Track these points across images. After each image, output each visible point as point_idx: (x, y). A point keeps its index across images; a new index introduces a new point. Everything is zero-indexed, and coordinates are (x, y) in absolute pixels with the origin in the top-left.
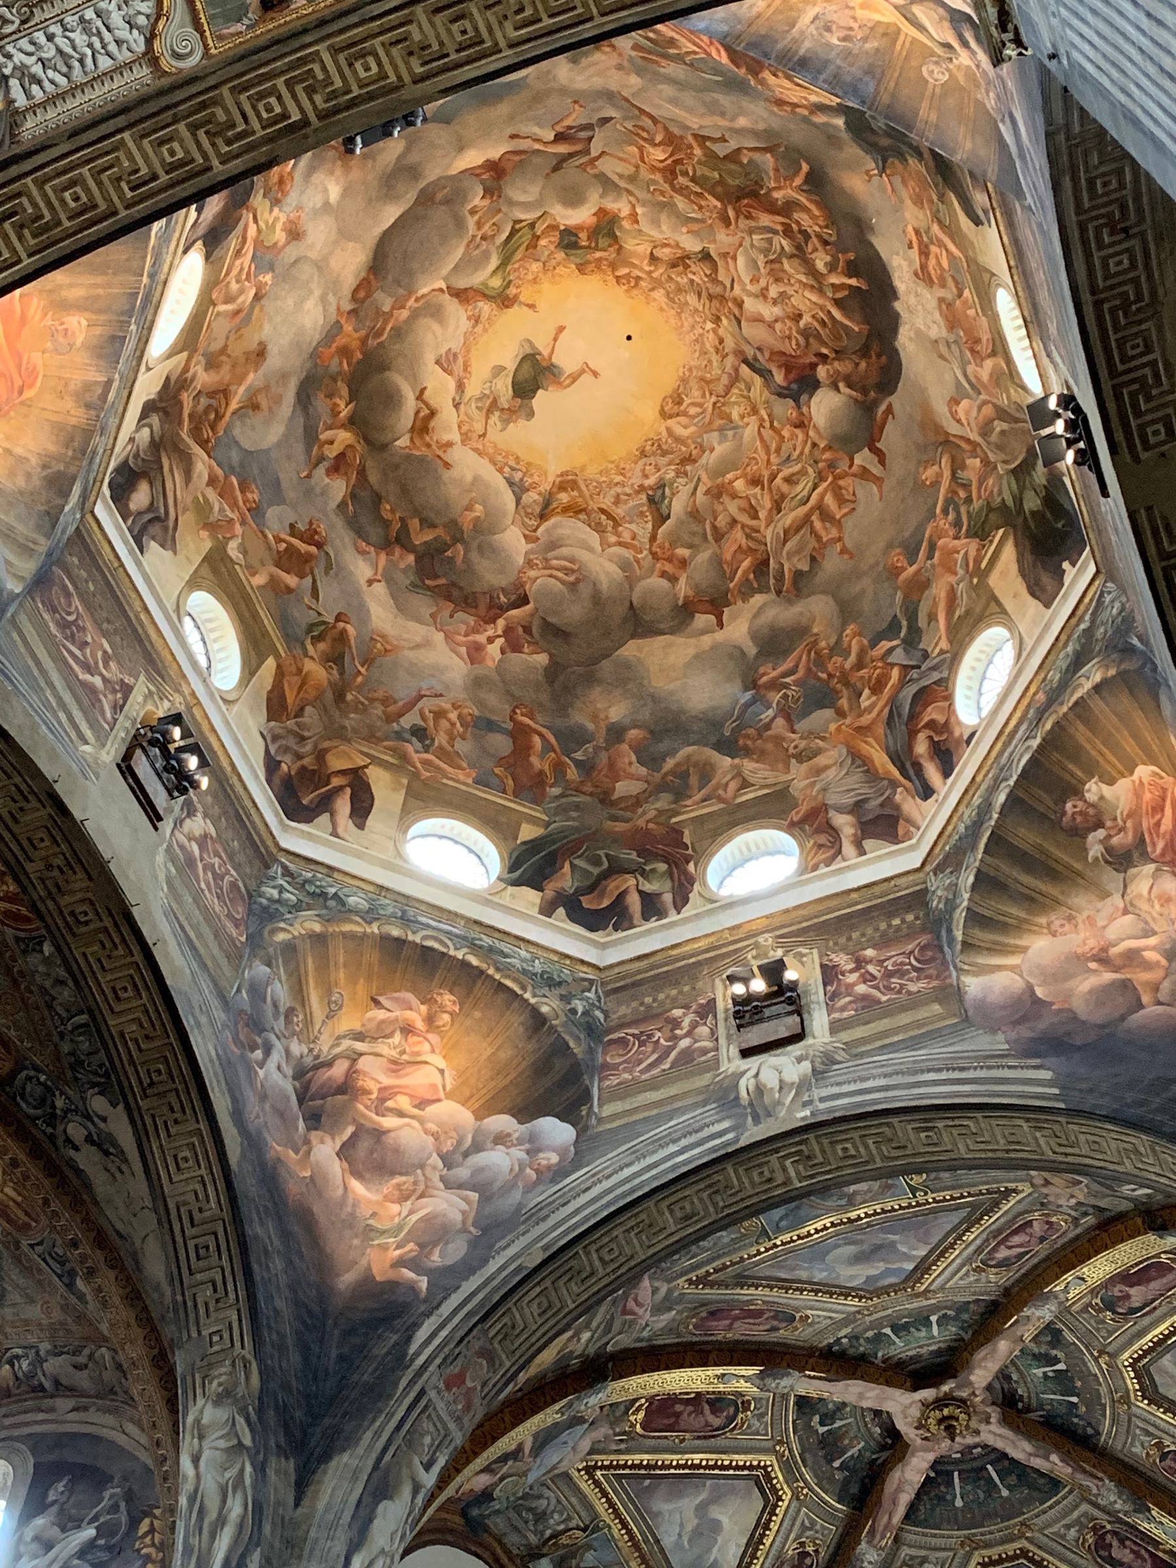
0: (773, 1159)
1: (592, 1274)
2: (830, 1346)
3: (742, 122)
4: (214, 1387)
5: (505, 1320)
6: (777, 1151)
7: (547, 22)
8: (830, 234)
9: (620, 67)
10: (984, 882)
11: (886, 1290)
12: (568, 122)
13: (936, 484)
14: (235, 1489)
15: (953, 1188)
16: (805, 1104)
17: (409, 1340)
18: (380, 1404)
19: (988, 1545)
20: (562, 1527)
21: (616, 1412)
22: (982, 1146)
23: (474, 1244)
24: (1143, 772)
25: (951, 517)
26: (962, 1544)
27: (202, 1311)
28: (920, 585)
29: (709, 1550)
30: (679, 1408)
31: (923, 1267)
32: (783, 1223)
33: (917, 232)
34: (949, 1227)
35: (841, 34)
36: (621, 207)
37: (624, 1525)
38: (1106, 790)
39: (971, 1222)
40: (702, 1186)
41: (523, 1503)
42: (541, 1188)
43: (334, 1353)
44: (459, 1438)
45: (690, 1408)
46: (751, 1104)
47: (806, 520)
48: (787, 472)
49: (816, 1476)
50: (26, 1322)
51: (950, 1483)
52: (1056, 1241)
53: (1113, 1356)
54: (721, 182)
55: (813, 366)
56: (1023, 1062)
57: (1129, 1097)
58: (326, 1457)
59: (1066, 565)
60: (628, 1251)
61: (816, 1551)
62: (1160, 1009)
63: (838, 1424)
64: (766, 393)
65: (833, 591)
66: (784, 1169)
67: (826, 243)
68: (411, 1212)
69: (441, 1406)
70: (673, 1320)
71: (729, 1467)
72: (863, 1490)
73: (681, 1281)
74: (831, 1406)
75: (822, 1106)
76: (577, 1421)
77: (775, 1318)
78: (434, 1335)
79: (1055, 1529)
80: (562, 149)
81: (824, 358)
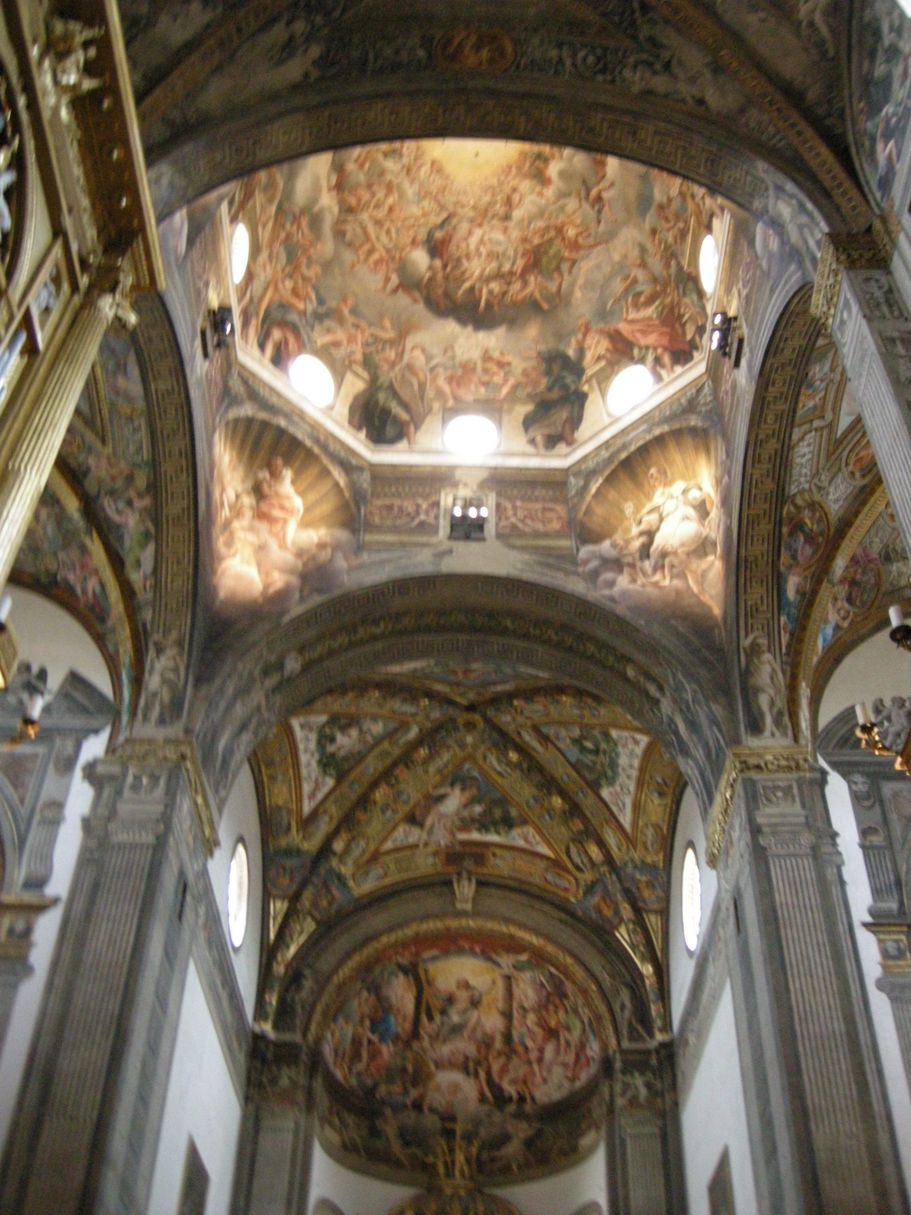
3: (578, 294)
7: (754, 491)
8: (508, 299)
9: (625, 256)
10: (250, 421)
12: (606, 208)
13: (383, 328)
25: (370, 340)
28: (341, 320)
33: (509, 364)
35: (655, 475)
36: (550, 192)
47: (368, 238)
48: (393, 230)
54: (546, 253)
55: (441, 257)
59: (364, 432)
64: (430, 225)
65: (337, 256)
67: (504, 294)
80: (594, 192)
81: (445, 266)
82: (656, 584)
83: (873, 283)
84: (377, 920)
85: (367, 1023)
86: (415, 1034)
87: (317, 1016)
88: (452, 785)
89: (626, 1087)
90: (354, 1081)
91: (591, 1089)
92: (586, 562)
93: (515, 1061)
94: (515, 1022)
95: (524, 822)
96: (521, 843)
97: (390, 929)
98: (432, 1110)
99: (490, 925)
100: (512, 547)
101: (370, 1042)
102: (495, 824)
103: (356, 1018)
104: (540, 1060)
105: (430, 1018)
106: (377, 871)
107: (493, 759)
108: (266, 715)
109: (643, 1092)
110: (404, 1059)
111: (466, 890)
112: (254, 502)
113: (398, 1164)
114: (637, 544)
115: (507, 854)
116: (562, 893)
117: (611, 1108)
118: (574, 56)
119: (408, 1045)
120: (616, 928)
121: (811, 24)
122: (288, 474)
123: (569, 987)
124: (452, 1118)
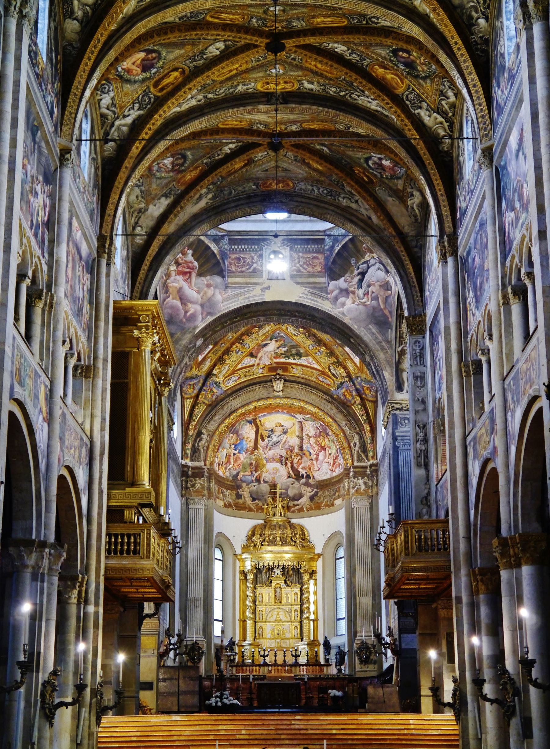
24: (196, 264)
38: (190, 255)
50: (151, 184)
82: (364, 304)
83: (417, 344)
84: (235, 402)
85: (233, 446)
86: (256, 447)
87: (210, 452)
88: (271, 340)
89: (356, 484)
90: (227, 474)
91: (339, 480)
92: (332, 291)
93: (305, 459)
94: (304, 441)
95: (307, 355)
96: (306, 364)
97: (243, 406)
98: (265, 482)
99: (290, 402)
100: (298, 283)
101: (234, 454)
102: (293, 355)
103: (228, 446)
104: (317, 459)
105: (263, 440)
106: (234, 378)
107: (291, 329)
108: (188, 363)
109: (363, 487)
110: (250, 459)
111: (278, 385)
112: (175, 268)
113: (250, 510)
114: (356, 279)
115: (300, 368)
116: (327, 386)
117: (348, 494)
118: (319, 189)
119: (252, 453)
120: (353, 405)
121: (412, 208)
122: (190, 252)
123: (330, 433)
124: (274, 486)
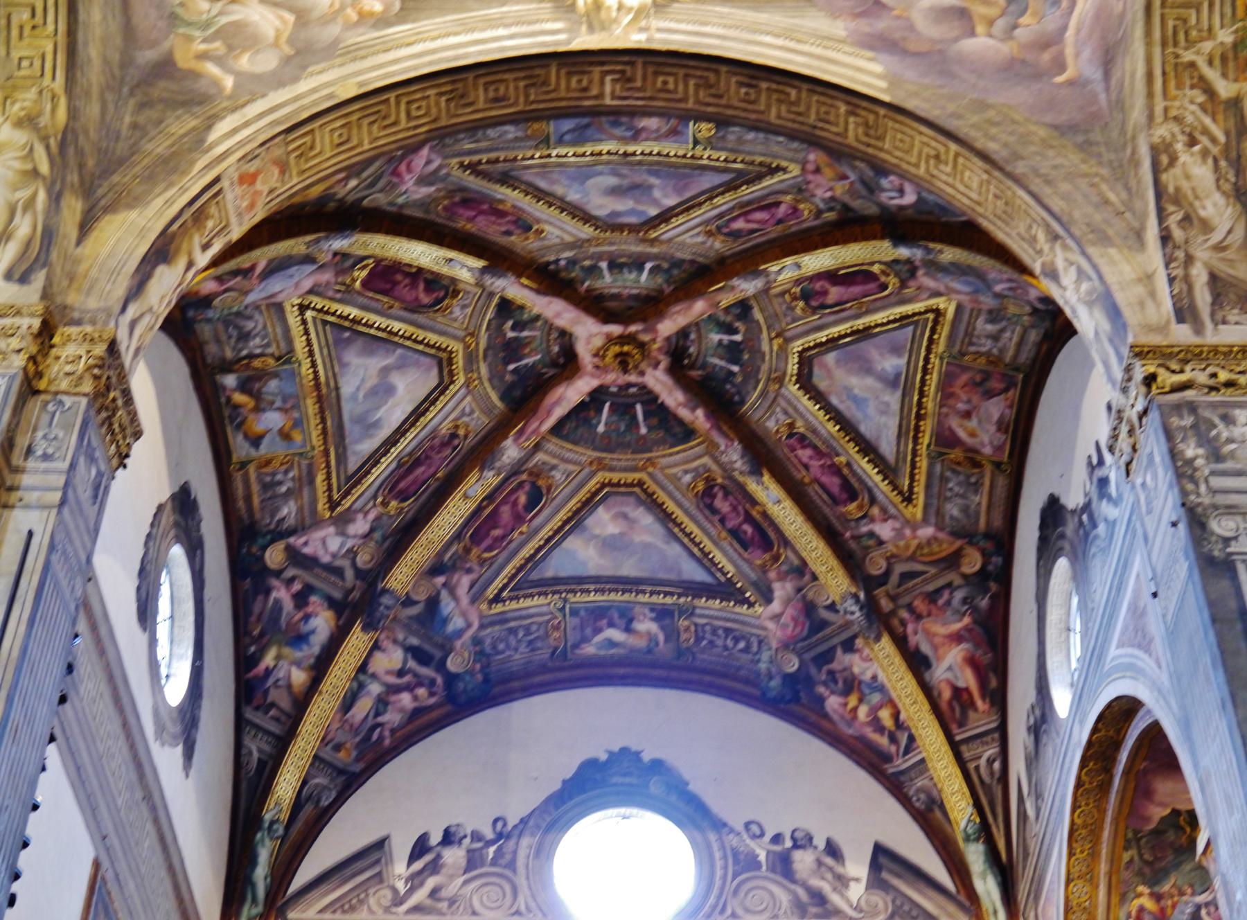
0: (597, 70)
1: (395, 124)
2: (548, 263)
4: (15, 109)
5: (307, 139)
6: (602, 64)
11: (620, 228)
14: (25, 210)
15: (732, 151)
16: (642, 30)
17: (209, 127)
18: (174, 177)
19: (612, 469)
20: (258, 351)
21: (344, 262)
22: (792, 116)
23: (287, 60)
26: (591, 463)
27: (15, 32)
29: (378, 408)
30: (399, 277)
31: (665, 216)
32: (567, 137)
34: (707, 185)
37: (314, 365)
39: (730, 187)
40: (522, 74)
41: (234, 320)
42: (361, 30)
43: (127, 119)
44: (236, 233)
45: (407, 281)
46: (587, 14)
49: (490, 371)
51: (600, 411)
52: (794, 226)
53: (788, 341)
56: (858, 51)
57: (951, 107)
58: (111, 208)
60: (434, 111)
61: (466, 437)
62: (991, 42)
63: (525, 334)
66: (602, 83)
68: (220, 14)
69: (229, 196)
70: (429, 196)
71: (421, 342)
72: (523, 396)
73: (454, 161)
74: (525, 316)
75: (658, 36)
76: (308, 259)
77: (515, 222)
78: (235, 131)
79: (674, 471)
